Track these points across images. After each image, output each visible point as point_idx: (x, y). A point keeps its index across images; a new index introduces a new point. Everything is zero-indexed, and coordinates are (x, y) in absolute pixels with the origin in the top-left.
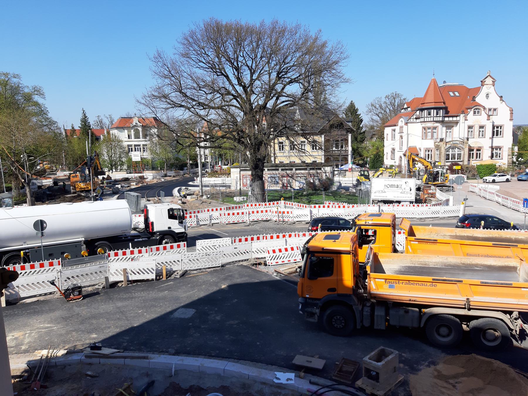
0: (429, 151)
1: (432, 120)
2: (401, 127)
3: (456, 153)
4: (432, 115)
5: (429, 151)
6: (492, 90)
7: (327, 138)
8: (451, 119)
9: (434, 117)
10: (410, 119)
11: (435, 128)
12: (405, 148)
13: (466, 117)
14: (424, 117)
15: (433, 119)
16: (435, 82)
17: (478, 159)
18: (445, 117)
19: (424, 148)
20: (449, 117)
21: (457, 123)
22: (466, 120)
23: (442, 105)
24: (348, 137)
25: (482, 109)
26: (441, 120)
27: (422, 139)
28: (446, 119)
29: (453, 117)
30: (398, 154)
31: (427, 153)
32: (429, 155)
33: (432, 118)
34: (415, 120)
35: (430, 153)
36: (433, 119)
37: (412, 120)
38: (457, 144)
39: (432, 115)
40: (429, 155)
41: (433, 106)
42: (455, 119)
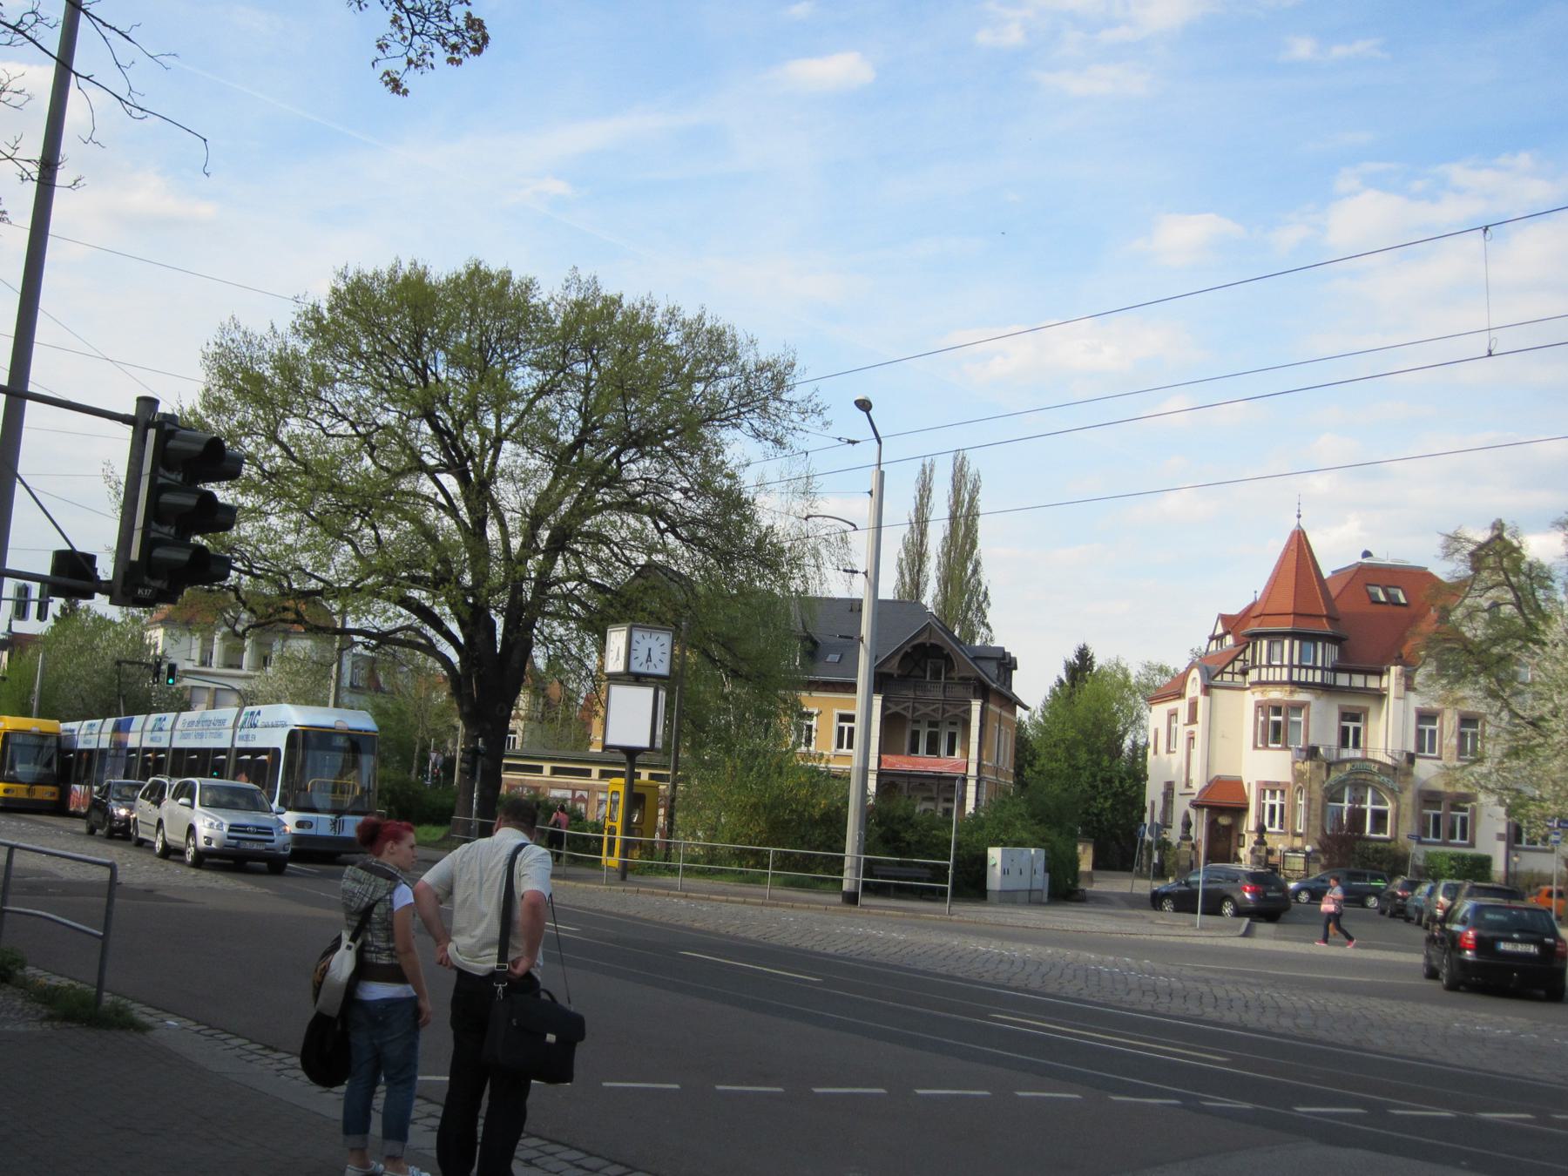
0: (1273, 793)
1: (1285, 678)
2: (1193, 706)
3: (1369, 806)
4: (1286, 662)
5: (1273, 793)
7: (894, 709)
8: (1358, 681)
9: (1291, 666)
10: (1222, 672)
11: (1298, 708)
12: (1198, 784)
16: (1300, 546)
17: (1458, 840)
18: (1336, 670)
19: (1259, 783)
20: (1351, 671)
21: (1379, 696)
23: (1326, 627)
24: (969, 711)
26: (1318, 679)
27: (1255, 747)
28: (1343, 680)
29: (1366, 672)
31: (1268, 801)
32: (1273, 807)
33: (1285, 671)
34: (1238, 678)
37: (1227, 677)
40: (1273, 807)
41: (1288, 628)
42: (1373, 683)
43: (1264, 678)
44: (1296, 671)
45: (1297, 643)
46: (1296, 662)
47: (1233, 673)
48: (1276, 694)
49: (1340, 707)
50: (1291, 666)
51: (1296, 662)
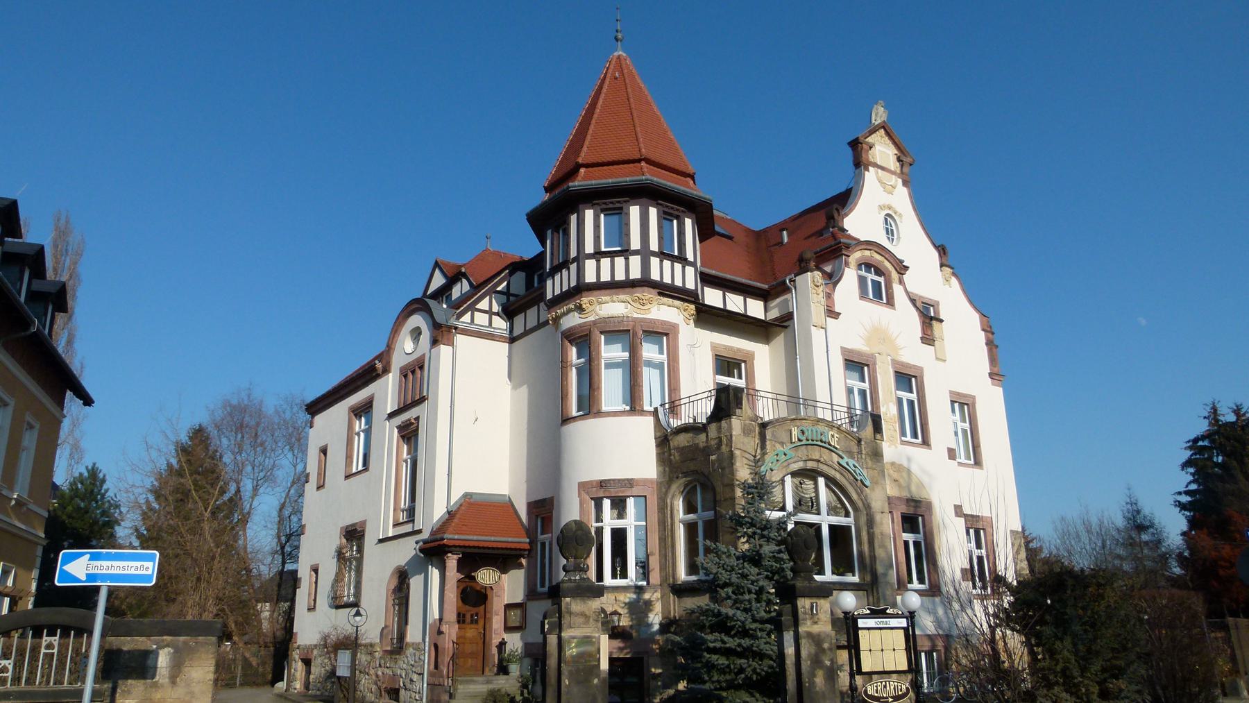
0: (619, 505)
1: (636, 274)
6: (901, 198)
8: (735, 303)
11: (661, 333)
13: (829, 296)
14: (580, 259)
15: (646, 267)
22: (832, 313)
25: (894, 275)
30: (379, 566)
32: (619, 537)
33: (635, 261)
35: (631, 522)
36: (646, 267)
37: (482, 319)
38: (832, 450)
39: (635, 244)
43: (590, 277)
44: (655, 262)
45: (653, 212)
46: (654, 247)
47: (490, 313)
48: (614, 307)
49: (714, 347)
50: (645, 253)
51: (654, 247)
